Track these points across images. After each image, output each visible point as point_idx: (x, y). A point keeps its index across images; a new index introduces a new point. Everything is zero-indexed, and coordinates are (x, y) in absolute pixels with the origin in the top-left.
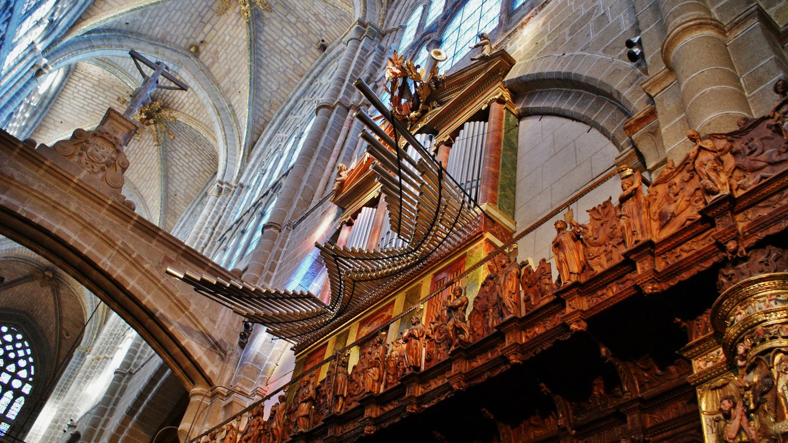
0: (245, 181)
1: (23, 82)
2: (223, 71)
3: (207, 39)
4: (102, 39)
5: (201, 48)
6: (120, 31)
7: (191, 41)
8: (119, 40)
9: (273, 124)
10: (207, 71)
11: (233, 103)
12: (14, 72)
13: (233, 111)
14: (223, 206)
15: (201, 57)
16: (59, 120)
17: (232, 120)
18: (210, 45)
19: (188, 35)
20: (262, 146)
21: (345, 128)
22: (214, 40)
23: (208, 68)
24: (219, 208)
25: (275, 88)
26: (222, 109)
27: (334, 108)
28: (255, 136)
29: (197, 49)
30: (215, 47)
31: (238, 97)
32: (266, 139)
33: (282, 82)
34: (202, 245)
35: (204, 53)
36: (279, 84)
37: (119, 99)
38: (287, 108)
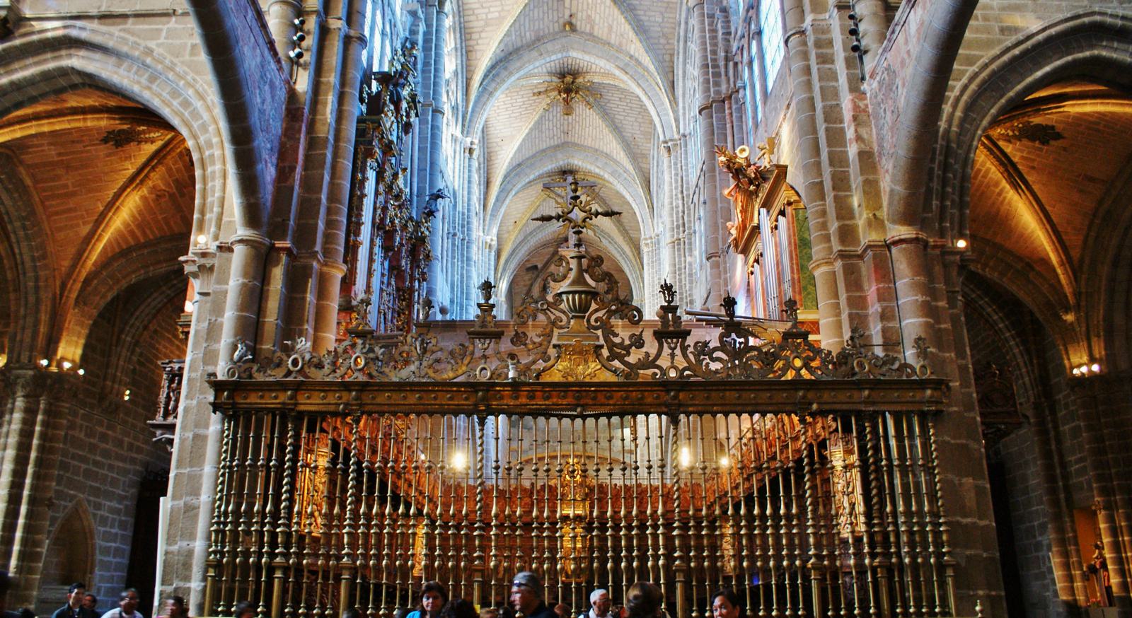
0: (685, 129)
1: (466, 171)
2: (606, 30)
3: (574, 11)
4: (493, 80)
5: (574, 21)
6: (501, 61)
7: (561, 21)
8: (506, 68)
9: (678, 53)
10: (591, 37)
11: (632, 53)
12: (457, 171)
13: (637, 60)
14: (679, 166)
15: (578, 28)
16: (499, 140)
17: (640, 70)
18: (580, 14)
19: (556, 19)
20: (681, 84)
21: (728, 126)
22: (580, 8)
23: (591, 34)
24: (676, 169)
25: (660, 20)
26: (627, 65)
27: (711, 106)
28: (670, 76)
29: (571, 24)
30: (585, 13)
31: (633, 46)
32: (680, 73)
33: (663, 10)
34: (681, 214)
35: (579, 24)
36: (662, 13)
37: (534, 94)
38: (682, 34)
